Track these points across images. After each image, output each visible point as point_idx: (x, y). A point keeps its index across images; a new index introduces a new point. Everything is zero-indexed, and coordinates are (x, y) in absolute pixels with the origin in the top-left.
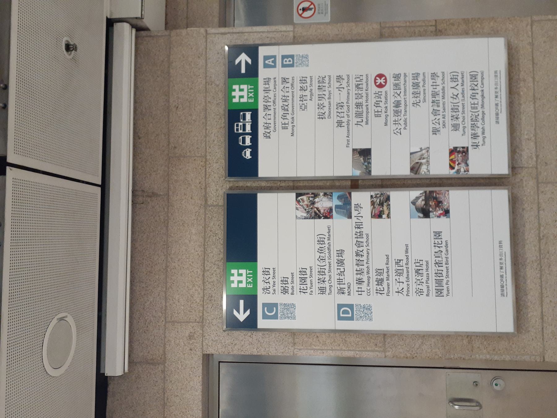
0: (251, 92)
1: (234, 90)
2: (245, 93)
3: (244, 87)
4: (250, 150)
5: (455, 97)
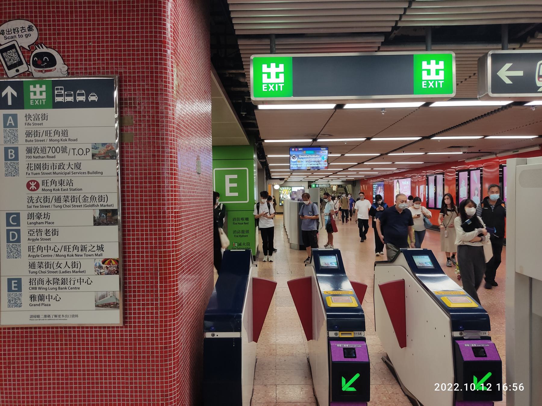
0: (39, 102)
2: (38, 96)
3: (44, 96)
5: (59, 265)
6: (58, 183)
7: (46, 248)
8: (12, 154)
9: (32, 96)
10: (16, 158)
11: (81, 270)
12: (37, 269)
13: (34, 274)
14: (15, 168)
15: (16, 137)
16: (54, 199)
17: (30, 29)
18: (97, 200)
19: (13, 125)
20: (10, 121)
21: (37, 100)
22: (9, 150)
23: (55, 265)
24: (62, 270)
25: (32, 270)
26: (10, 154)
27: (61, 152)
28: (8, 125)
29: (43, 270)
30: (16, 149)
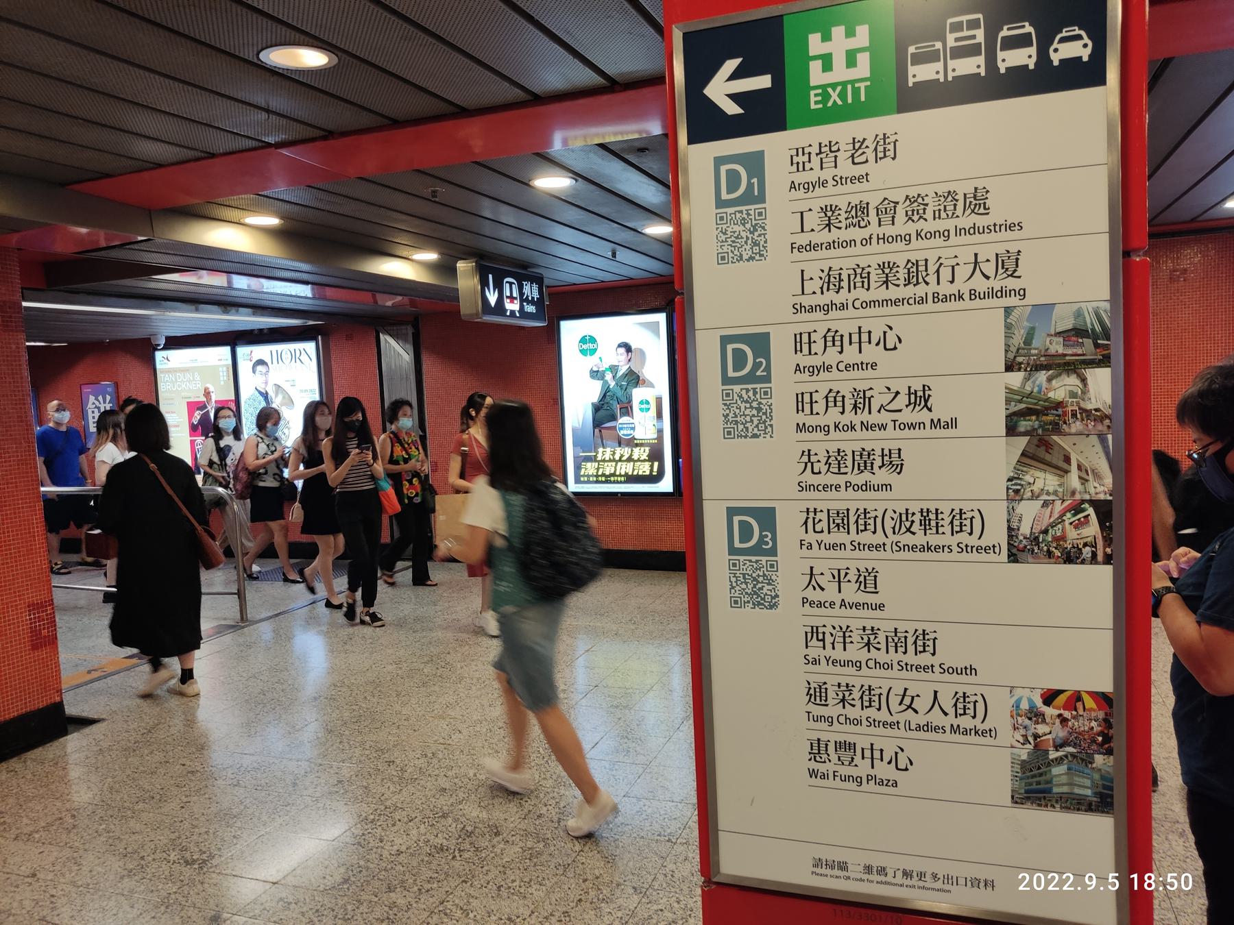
0: (843, 95)
1: (850, 33)
2: (841, 73)
4: (1085, 54)
5: (907, 701)
7: (855, 338)
9: (817, 76)
11: (981, 727)
12: (833, 710)
13: (824, 725)
21: (834, 86)
23: (894, 701)
24: (915, 719)
25: (818, 711)
29: (853, 713)
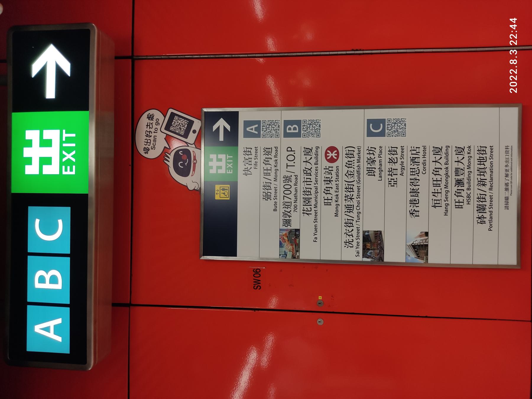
6: (328, 186)
8: (292, 128)
10: (298, 123)
14: (310, 124)
15: (272, 123)
16: (348, 214)
17: (150, 117)
18: (352, 159)
19: (257, 126)
20: (252, 129)
22: (288, 131)
26: (292, 131)
27: (290, 183)
28: (257, 133)
30: (287, 123)
